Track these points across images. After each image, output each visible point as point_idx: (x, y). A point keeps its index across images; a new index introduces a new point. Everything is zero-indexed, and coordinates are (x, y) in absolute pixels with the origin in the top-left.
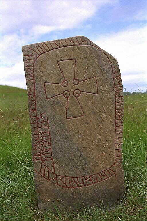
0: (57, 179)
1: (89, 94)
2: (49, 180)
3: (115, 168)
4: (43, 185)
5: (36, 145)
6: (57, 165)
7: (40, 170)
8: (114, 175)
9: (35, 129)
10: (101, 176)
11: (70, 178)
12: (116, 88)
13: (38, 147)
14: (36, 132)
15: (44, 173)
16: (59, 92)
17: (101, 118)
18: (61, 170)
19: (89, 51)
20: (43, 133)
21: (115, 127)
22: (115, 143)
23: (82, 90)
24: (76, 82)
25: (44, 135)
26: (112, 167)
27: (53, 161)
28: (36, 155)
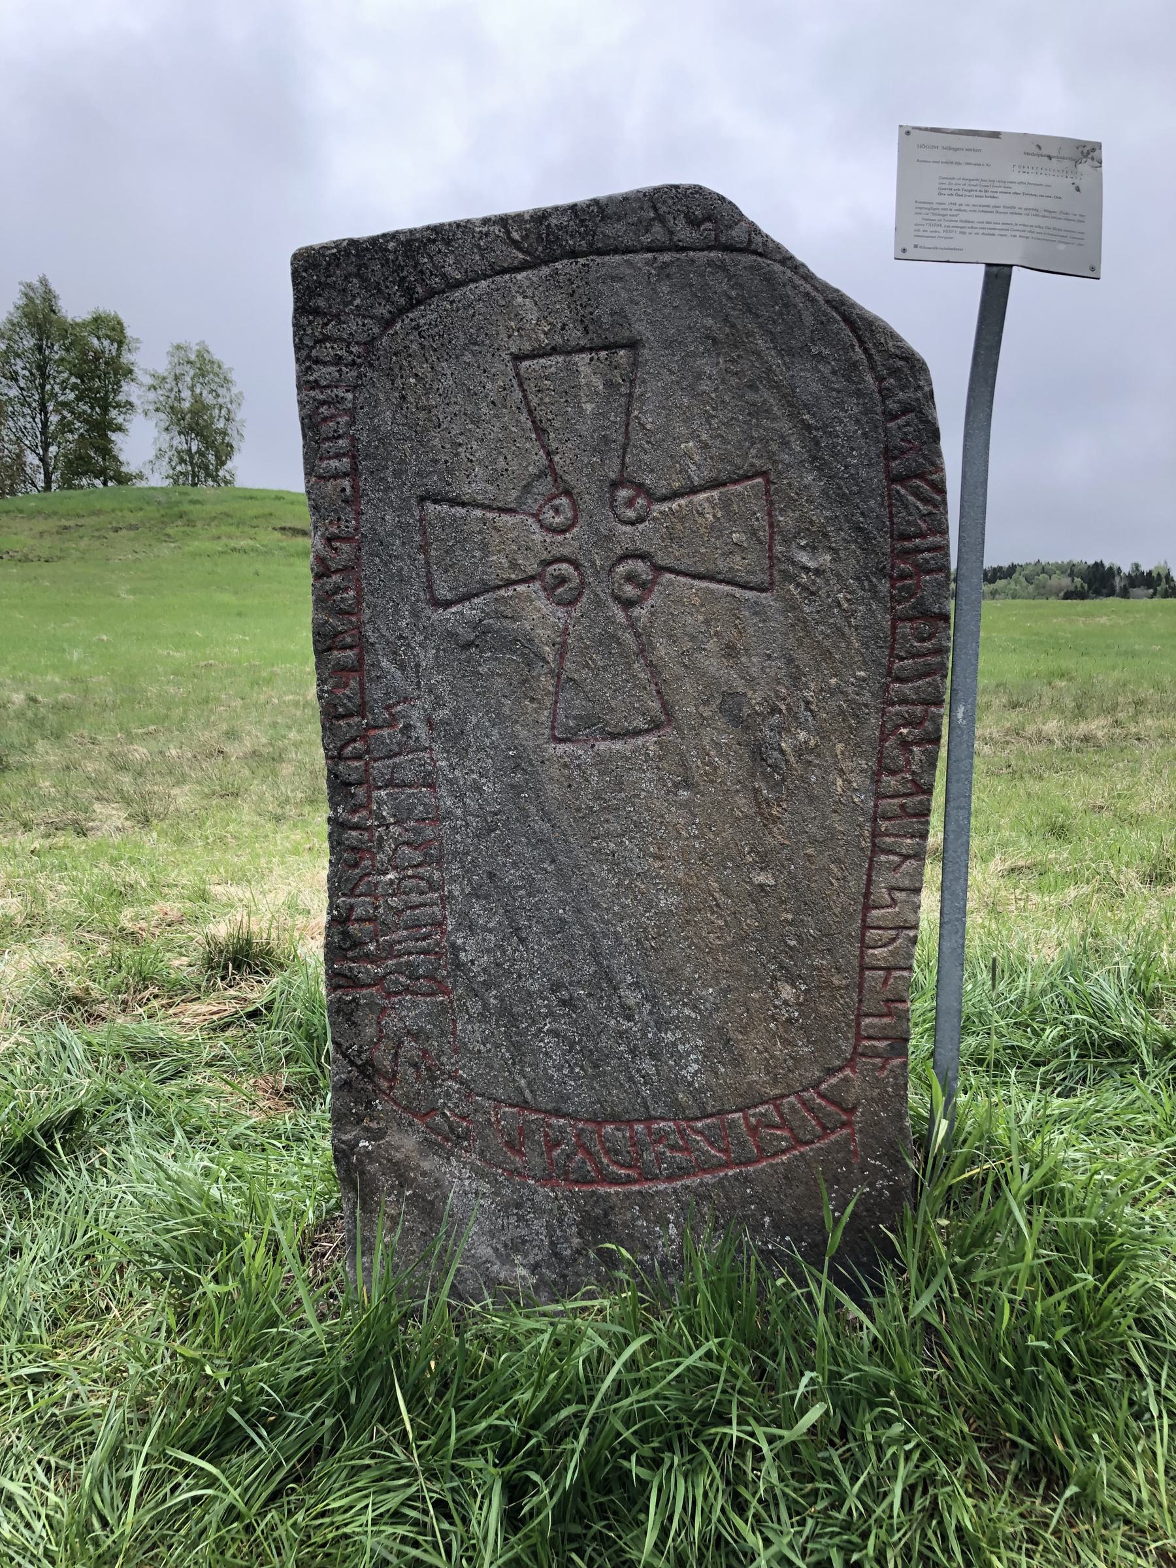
1: (712, 592)
10: (753, 1130)
12: (906, 553)
16: (514, 565)
17: (782, 752)
19: (733, 293)
23: (667, 562)
24: (630, 503)
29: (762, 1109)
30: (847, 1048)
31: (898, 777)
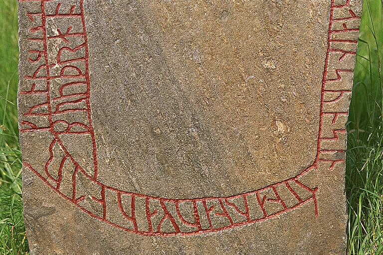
0: (103, 200)
2: (73, 200)
3: (317, 176)
4: (52, 219)
5: (34, 76)
6: (106, 153)
7: (44, 164)
8: (312, 200)
9: (31, 19)
11: (151, 200)
13: (40, 84)
14: (36, 29)
15: (60, 175)
18: (119, 169)
20: (61, 35)
21: (330, 32)
22: (323, 90)
25: (65, 44)
26: (306, 174)
27: (93, 136)
28: (35, 110)
29: (266, 190)
30: (313, 155)
31: (343, 8)
